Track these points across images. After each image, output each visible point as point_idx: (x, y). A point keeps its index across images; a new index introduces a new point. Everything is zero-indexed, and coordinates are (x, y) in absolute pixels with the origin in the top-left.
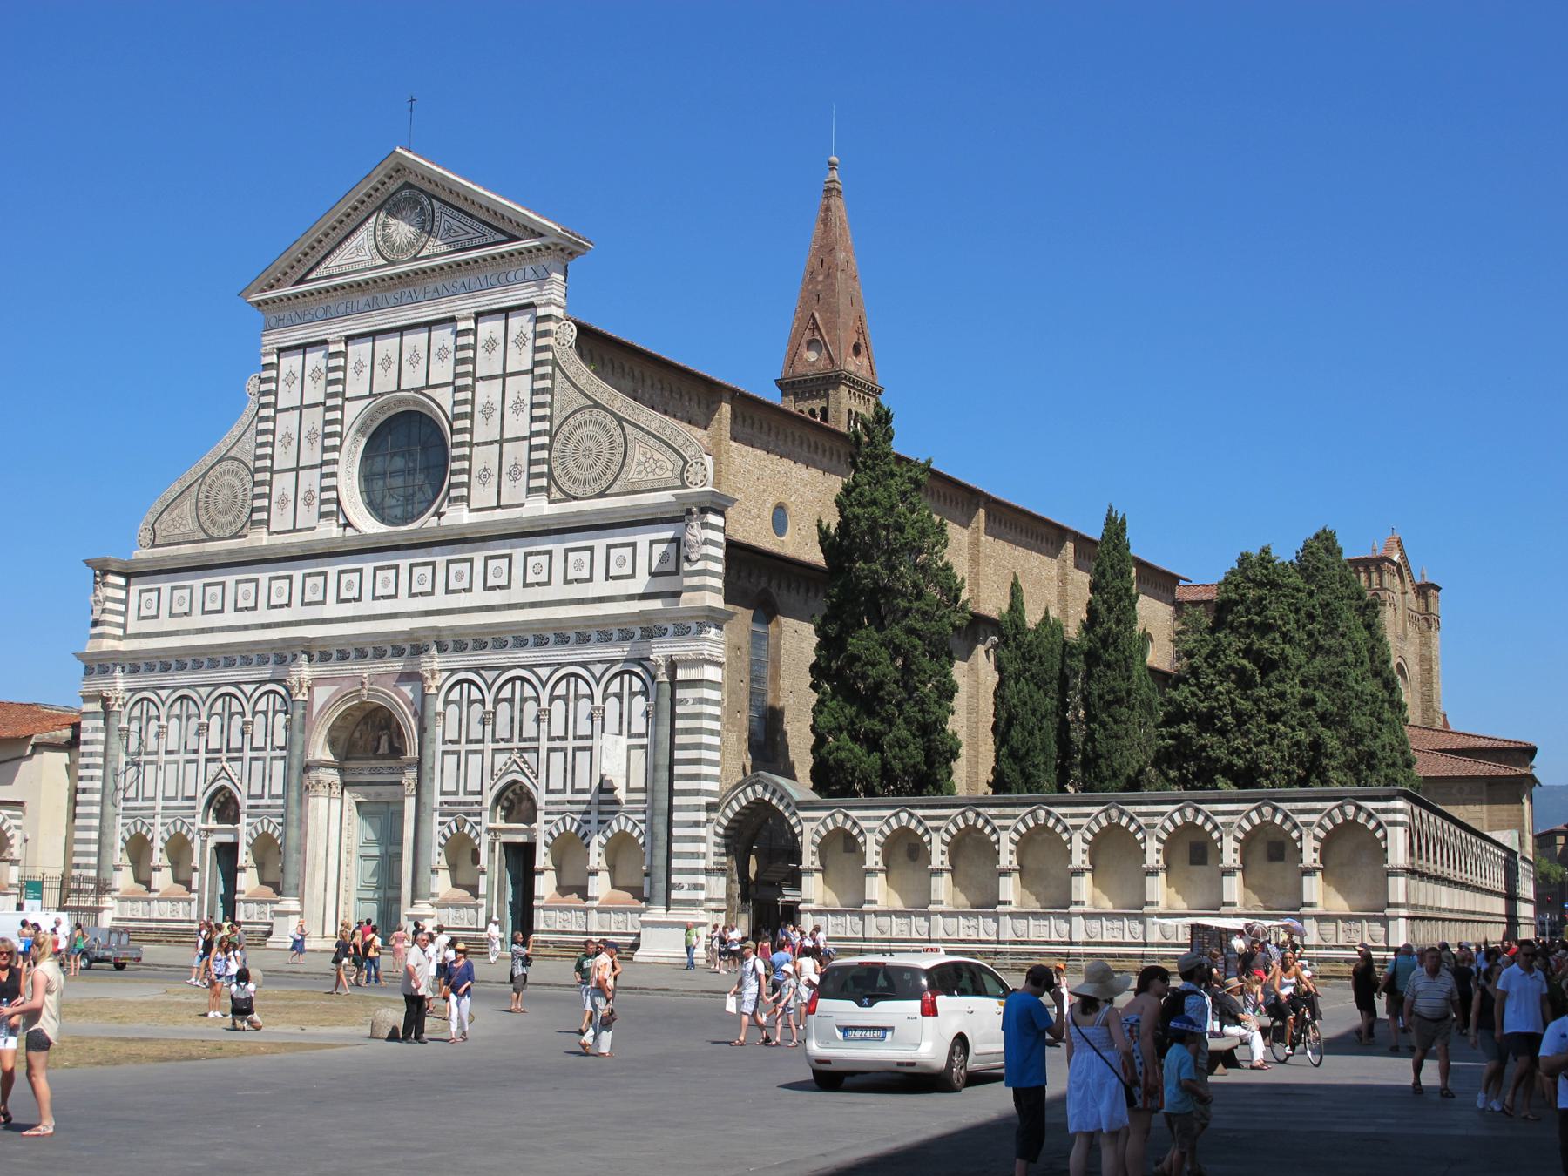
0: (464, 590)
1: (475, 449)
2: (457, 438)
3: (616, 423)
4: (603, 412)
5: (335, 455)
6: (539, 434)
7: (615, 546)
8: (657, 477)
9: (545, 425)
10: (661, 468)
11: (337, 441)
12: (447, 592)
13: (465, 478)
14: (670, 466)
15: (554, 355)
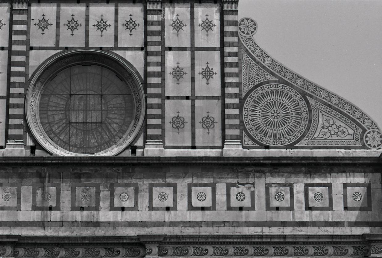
0: (168, 209)
1: (167, 102)
2: (150, 91)
3: (300, 96)
4: (288, 87)
5: (22, 91)
6: (231, 96)
7: (313, 185)
8: (339, 138)
9: (236, 90)
10: (343, 132)
11: (22, 79)
12: (151, 208)
13: (158, 122)
14: (351, 132)
15: (239, 39)
